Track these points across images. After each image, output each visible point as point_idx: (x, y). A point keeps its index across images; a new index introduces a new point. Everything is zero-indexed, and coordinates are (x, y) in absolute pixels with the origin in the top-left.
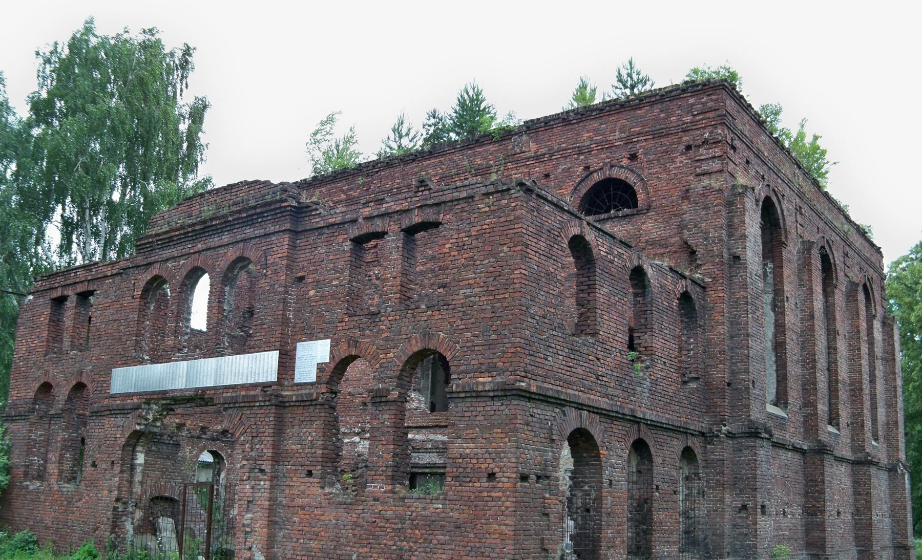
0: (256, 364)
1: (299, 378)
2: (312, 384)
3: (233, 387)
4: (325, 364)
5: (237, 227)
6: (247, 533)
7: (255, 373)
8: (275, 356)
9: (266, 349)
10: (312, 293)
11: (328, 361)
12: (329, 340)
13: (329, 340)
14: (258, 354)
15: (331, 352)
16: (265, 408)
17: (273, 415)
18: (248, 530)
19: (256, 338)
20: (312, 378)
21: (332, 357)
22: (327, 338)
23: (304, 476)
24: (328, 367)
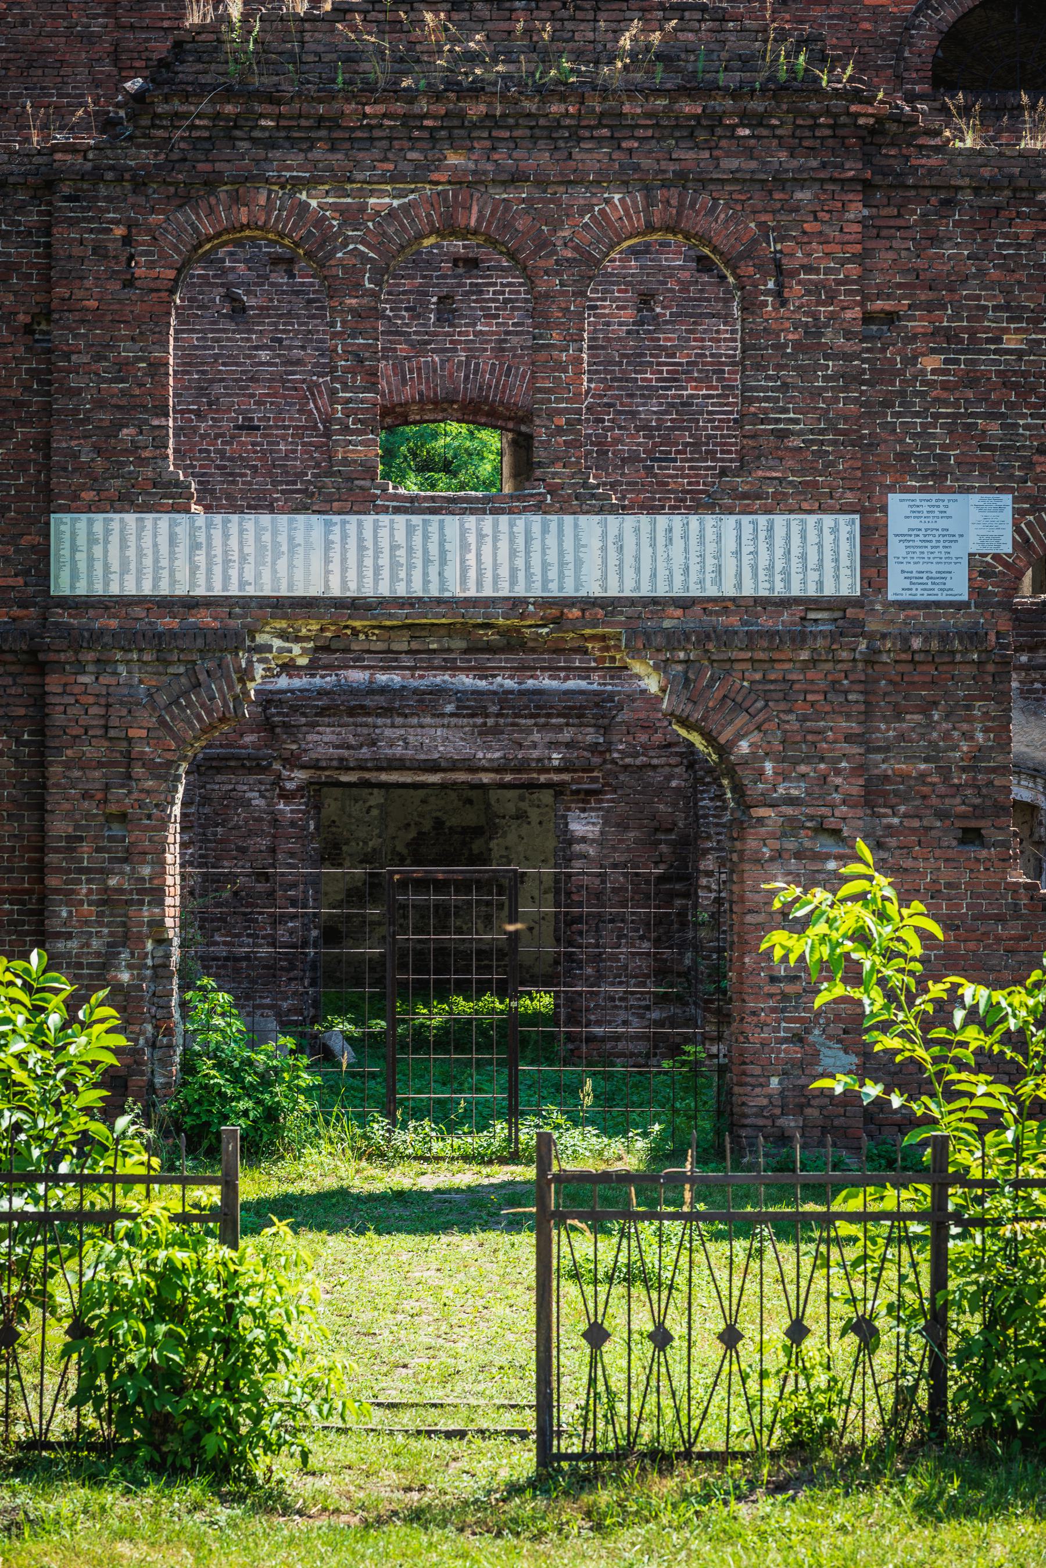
0: (771, 548)
1: (897, 588)
2: (959, 606)
3: (685, 604)
4: (996, 557)
5: (640, 133)
6: (785, 997)
7: (771, 568)
8: (844, 531)
9: (805, 506)
10: (931, 363)
11: (1006, 548)
12: (1007, 499)
13: (1007, 499)
14: (779, 520)
15: (1018, 530)
16: (829, 666)
17: (860, 687)
18: (790, 989)
19: (760, 473)
20: (959, 588)
21: (1022, 544)
22: (1000, 490)
23: (954, 843)
24: (1005, 564)
